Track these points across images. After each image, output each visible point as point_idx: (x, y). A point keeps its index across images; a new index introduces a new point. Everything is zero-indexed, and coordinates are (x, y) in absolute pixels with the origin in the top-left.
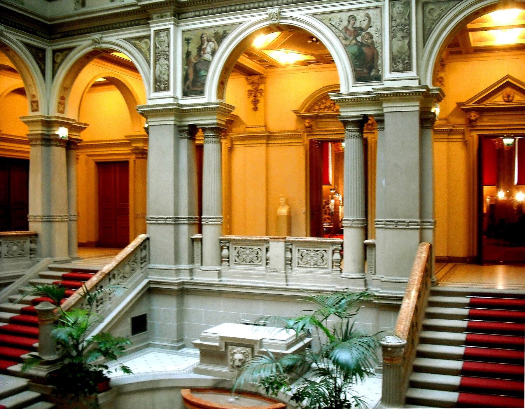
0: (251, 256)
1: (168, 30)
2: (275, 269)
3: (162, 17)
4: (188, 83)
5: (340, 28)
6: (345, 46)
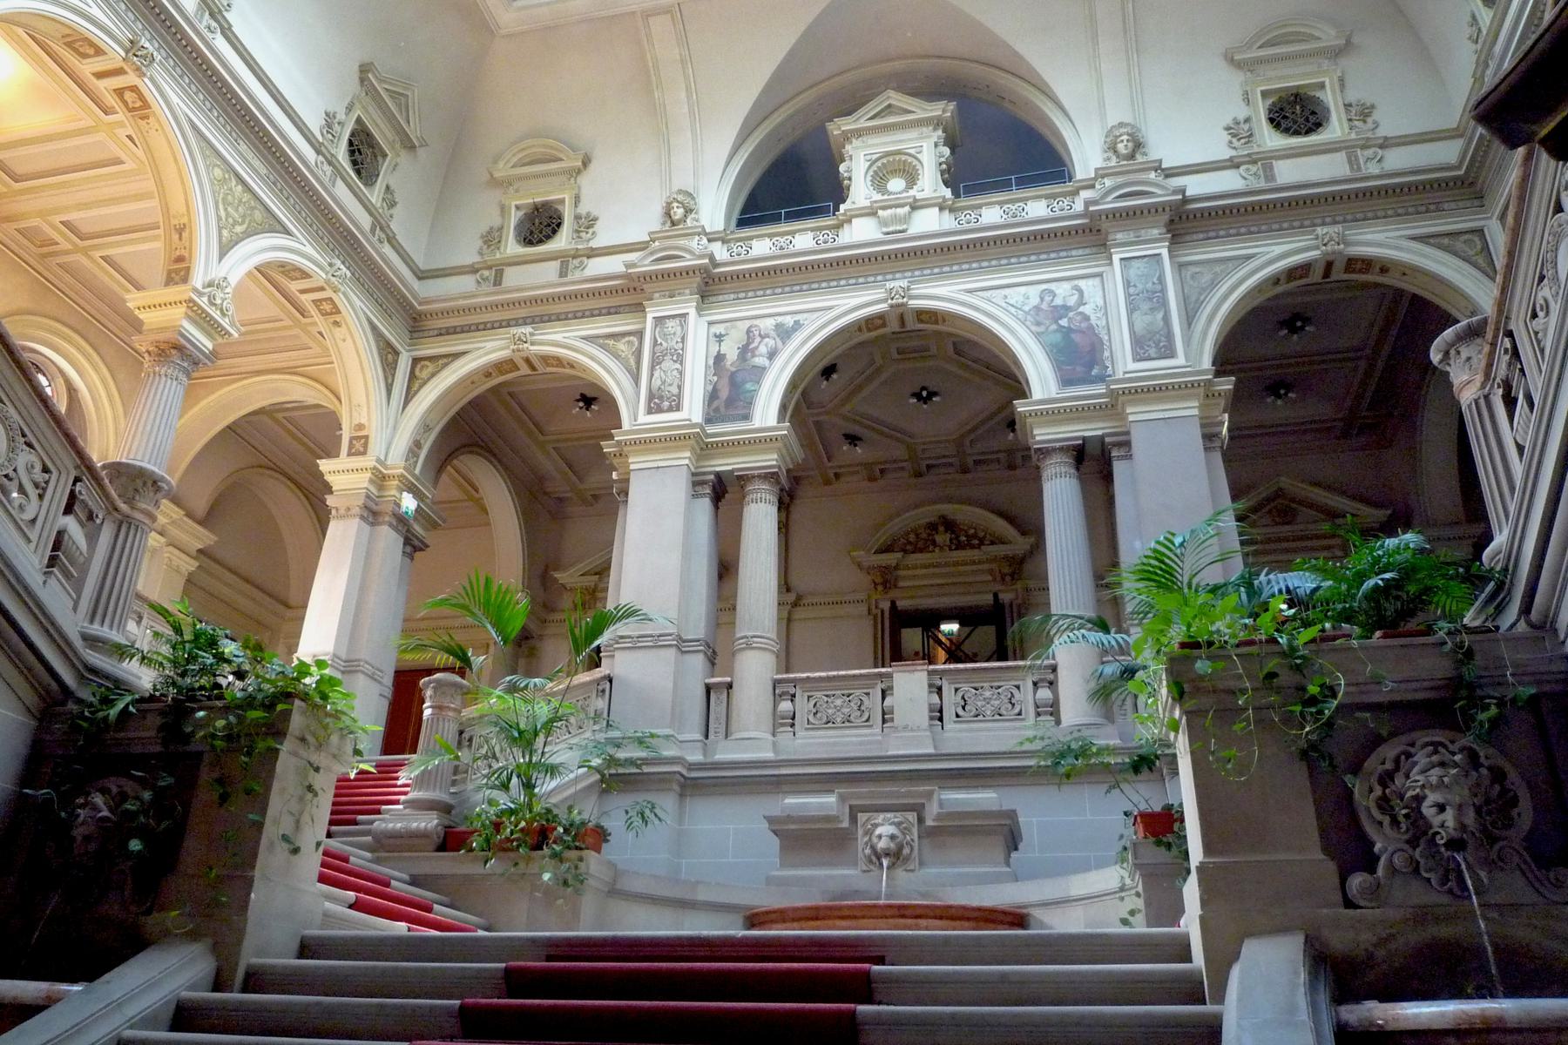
0: (846, 710)
1: (684, 315)
2: (905, 728)
4: (716, 404)
5: (1026, 308)
6: (1037, 335)
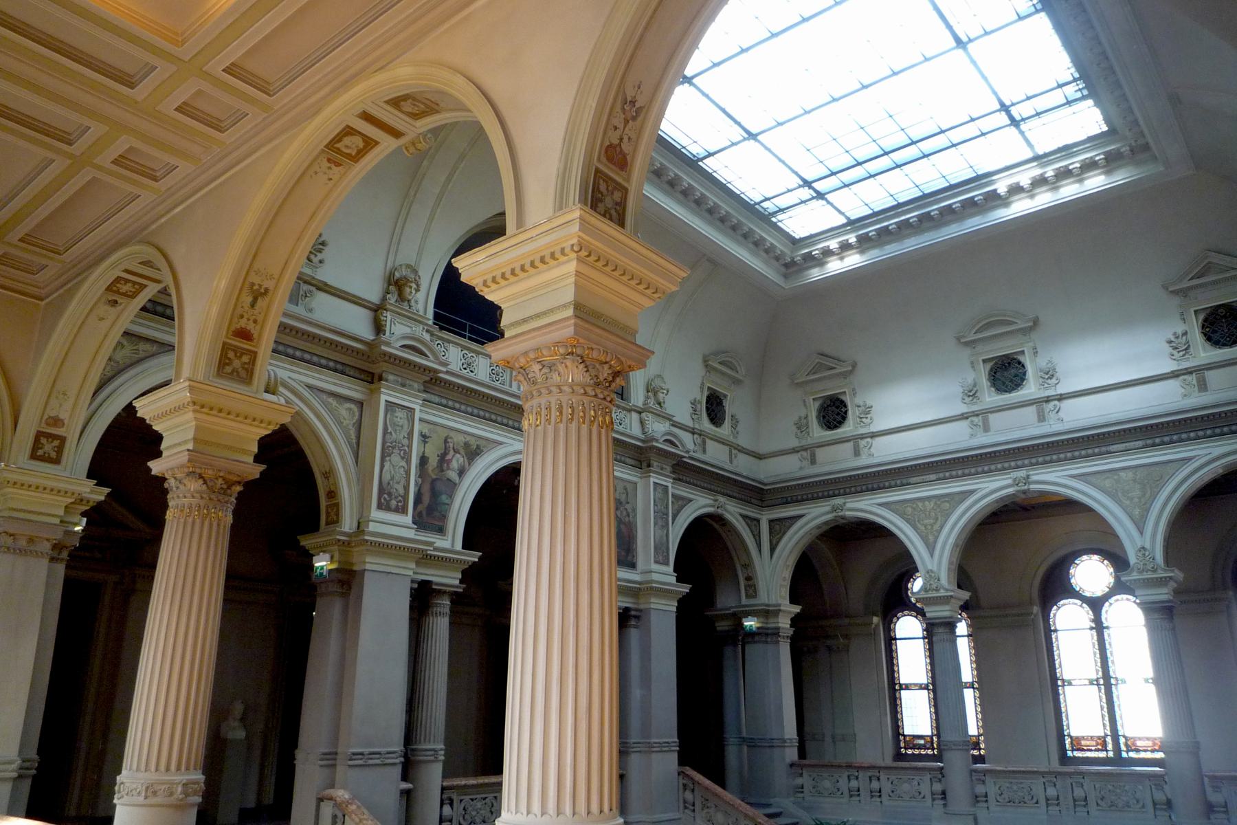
3: (403, 385)
4: (420, 508)
